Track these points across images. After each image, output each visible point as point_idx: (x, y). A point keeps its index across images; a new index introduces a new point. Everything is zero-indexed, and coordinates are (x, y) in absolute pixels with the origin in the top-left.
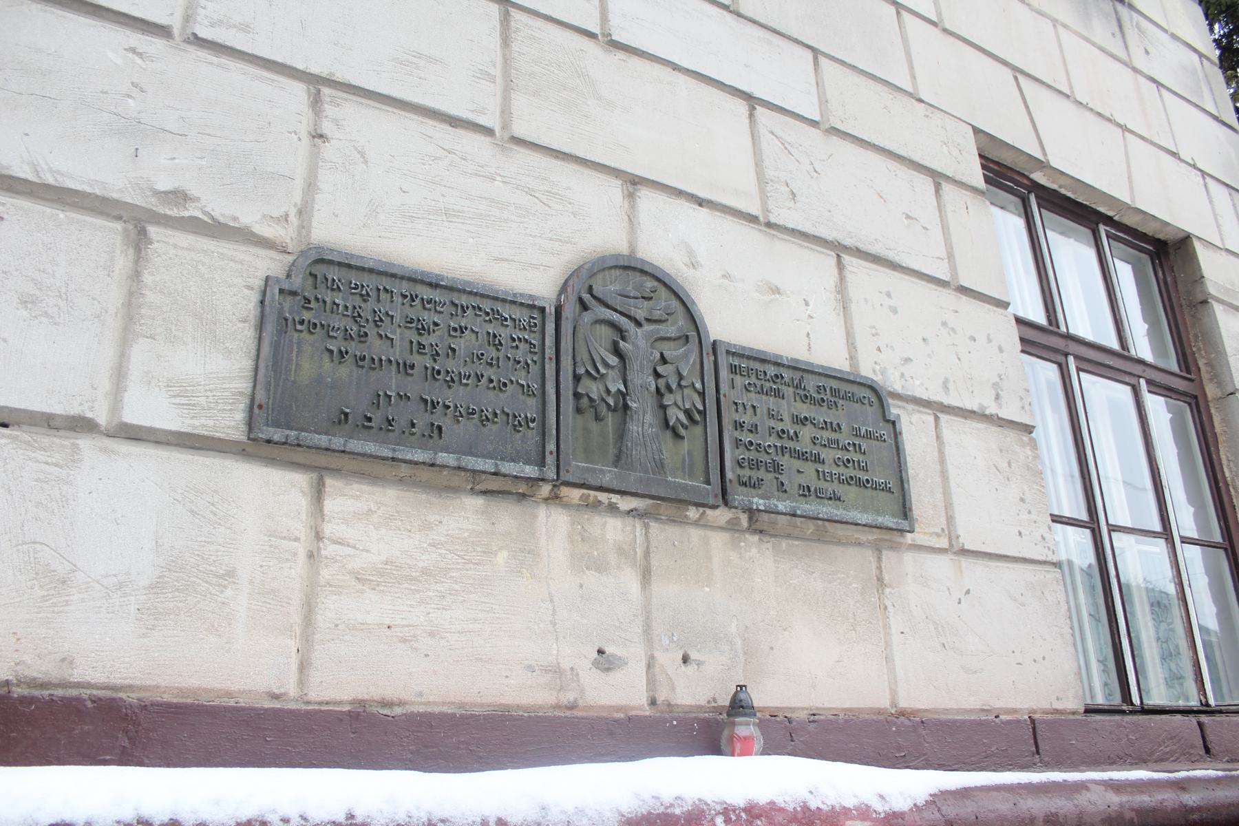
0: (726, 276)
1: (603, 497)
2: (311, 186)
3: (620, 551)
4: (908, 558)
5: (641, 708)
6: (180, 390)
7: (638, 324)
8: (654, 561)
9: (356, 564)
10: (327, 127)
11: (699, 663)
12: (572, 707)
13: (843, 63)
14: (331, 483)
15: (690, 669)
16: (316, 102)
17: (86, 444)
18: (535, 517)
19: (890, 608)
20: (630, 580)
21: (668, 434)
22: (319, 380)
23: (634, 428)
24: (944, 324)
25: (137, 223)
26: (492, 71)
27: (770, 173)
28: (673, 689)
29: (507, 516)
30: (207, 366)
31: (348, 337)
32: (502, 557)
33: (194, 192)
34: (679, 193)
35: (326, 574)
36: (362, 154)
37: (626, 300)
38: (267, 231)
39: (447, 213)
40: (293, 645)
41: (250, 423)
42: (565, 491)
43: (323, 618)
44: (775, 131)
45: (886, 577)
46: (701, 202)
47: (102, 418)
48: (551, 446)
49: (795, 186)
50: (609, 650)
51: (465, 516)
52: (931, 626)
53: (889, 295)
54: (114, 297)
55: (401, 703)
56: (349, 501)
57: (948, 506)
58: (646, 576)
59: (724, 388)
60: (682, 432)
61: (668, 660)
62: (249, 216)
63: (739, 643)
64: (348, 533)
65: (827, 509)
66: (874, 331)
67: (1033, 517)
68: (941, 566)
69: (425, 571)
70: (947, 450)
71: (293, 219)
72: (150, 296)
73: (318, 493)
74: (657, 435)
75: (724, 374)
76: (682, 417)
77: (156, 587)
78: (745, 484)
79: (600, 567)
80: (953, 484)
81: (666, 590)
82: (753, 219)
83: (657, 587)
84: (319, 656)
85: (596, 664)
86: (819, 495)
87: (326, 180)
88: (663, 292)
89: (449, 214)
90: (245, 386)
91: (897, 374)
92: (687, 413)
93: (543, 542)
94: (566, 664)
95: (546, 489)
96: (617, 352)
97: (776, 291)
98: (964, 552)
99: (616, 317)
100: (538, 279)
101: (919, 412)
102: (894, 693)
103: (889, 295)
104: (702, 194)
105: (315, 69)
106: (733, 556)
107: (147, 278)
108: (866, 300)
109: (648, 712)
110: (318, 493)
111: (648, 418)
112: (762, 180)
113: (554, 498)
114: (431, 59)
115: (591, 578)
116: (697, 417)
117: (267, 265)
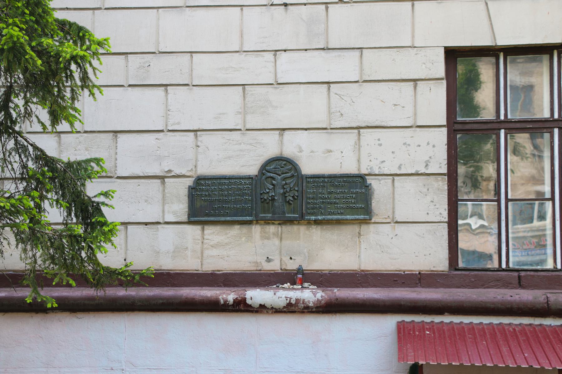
0: (312, 152)
2: (197, 160)
3: (274, 234)
4: (372, 227)
6: (174, 213)
7: (280, 175)
8: (283, 235)
9: (211, 244)
10: (199, 144)
11: (294, 259)
12: (260, 270)
13: (375, 48)
14: (206, 227)
15: (291, 261)
16: (196, 136)
17: (159, 226)
18: (252, 228)
19: (362, 242)
20: (276, 241)
21: (287, 204)
22: (201, 206)
23: (276, 204)
24: (405, 144)
25: (162, 178)
26: (240, 111)
27: (332, 110)
28: (287, 266)
29: (245, 229)
30: (179, 208)
31: (206, 196)
32: (243, 239)
33: (172, 169)
35: (205, 246)
36: (207, 148)
38: (188, 174)
39: (229, 158)
40: (199, 261)
41: (189, 218)
42: (259, 222)
43: (205, 255)
44: (337, 93)
45: (362, 233)
46: (306, 129)
47: (161, 222)
48: (254, 212)
49: (342, 112)
51: (236, 230)
52: (378, 246)
53: (379, 140)
54: (160, 196)
56: (210, 230)
57: (393, 208)
58: (281, 239)
59: (304, 188)
60: (291, 202)
61: (286, 259)
62: (184, 172)
63: (307, 254)
64: (210, 237)
65: (339, 217)
67: (436, 207)
69: (226, 244)
70: (396, 190)
71: (194, 169)
72: (167, 195)
73: (203, 230)
74: (283, 205)
75: (304, 184)
76: (291, 198)
77: (174, 252)
78: (309, 214)
79: (268, 238)
80: (396, 201)
81: (286, 243)
82: (326, 129)
83: (283, 242)
84: (204, 262)
85: (266, 261)
86: (333, 214)
87: (200, 157)
88: (288, 164)
89: (229, 158)
90: (187, 210)
91: (377, 168)
92: (293, 197)
94: (259, 261)
95: (255, 222)
96: (273, 185)
97: (330, 151)
98: (397, 222)
99: (272, 175)
100: (252, 170)
102: (360, 265)
103: (379, 140)
104: (305, 127)
105: (195, 129)
106: (307, 232)
107: (166, 191)
108: (368, 145)
110: (203, 230)
111: (280, 200)
112: (330, 113)
113: (257, 223)
114: (224, 114)
115: (266, 241)
116: (296, 197)
117: (189, 182)
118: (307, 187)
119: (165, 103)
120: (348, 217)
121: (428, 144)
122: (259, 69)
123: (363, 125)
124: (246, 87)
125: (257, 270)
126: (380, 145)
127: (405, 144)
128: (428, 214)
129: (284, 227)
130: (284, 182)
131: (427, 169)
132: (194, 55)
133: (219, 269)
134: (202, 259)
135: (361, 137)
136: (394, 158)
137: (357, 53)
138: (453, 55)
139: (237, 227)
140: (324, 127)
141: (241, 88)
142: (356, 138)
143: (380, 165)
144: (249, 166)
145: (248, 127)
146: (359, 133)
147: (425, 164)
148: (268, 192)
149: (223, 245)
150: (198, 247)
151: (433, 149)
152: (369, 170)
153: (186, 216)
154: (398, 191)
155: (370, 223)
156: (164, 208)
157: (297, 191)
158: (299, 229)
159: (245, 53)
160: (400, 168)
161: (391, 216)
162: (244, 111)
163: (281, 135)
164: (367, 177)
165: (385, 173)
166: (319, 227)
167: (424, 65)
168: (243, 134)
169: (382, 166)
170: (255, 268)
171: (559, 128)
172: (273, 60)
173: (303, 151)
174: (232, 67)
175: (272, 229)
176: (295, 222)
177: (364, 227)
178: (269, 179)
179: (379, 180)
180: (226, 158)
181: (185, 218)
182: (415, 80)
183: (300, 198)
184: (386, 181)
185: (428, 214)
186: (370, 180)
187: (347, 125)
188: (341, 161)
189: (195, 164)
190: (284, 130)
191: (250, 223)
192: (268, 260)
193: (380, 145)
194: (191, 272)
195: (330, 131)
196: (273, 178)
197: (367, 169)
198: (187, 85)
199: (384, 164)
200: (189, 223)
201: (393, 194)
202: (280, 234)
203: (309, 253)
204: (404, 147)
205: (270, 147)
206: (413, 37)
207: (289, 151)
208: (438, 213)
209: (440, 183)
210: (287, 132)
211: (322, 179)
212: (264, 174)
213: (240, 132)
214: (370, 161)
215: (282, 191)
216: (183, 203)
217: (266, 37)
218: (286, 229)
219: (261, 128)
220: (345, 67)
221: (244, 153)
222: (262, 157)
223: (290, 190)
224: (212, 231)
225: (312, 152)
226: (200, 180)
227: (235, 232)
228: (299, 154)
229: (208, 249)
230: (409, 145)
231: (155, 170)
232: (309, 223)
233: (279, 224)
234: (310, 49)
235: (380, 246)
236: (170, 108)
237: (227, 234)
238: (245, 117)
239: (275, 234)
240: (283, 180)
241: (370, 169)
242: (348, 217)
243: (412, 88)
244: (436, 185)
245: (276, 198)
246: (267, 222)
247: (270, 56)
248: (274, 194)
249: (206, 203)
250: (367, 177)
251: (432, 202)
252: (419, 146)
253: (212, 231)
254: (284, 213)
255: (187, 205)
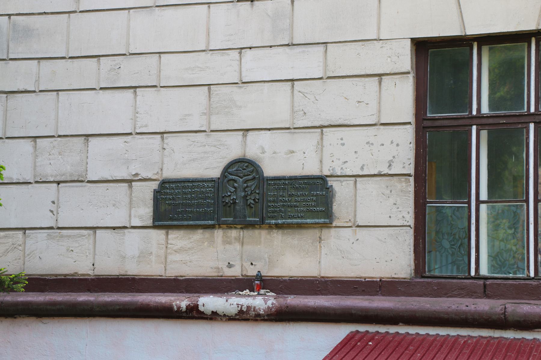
1: (232, 226)
2: (163, 164)
3: (235, 239)
4: (333, 231)
5: (239, 276)
6: (141, 217)
7: (241, 178)
8: (245, 240)
9: (175, 248)
10: (165, 146)
11: (255, 265)
12: (222, 276)
13: (340, 42)
14: (170, 232)
15: (251, 267)
16: (163, 138)
17: (126, 231)
18: (214, 233)
19: (323, 247)
20: (238, 246)
24: (368, 143)
25: (129, 182)
26: (205, 112)
27: (296, 109)
28: (247, 271)
29: (207, 233)
30: (144, 212)
32: (206, 244)
33: (139, 173)
34: (262, 129)
35: (169, 251)
36: (173, 150)
37: (243, 169)
39: (194, 160)
40: (163, 266)
41: (153, 222)
42: (221, 226)
43: (168, 260)
44: (301, 90)
45: (323, 238)
46: (269, 129)
47: (128, 226)
48: (216, 216)
50: (231, 263)
51: (198, 235)
52: (339, 252)
53: (342, 139)
54: (127, 200)
55: (184, 276)
56: (174, 235)
57: (355, 211)
59: (265, 190)
60: (253, 206)
61: (247, 265)
62: (150, 175)
63: (267, 260)
65: (299, 221)
66: (332, 155)
68: (347, 232)
69: (189, 248)
70: (358, 192)
71: (160, 172)
72: (134, 199)
73: (167, 234)
75: (265, 187)
76: (252, 202)
77: (139, 257)
78: (269, 217)
79: (230, 243)
80: (358, 203)
82: (289, 128)
83: (245, 247)
85: (227, 266)
87: (166, 160)
88: (250, 166)
89: (194, 160)
90: (152, 214)
91: (339, 169)
92: (254, 200)
93: (216, 239)
94: (220, 267)
96: (235, 188)
97: (293, 152)
98: (358, 226)
99: (234, 177)
100: (215, 173)
101: (346, 180)
102: (320, 271)
103: (342, 139)
104: (268, 127)
105: (162, 131)
106: (268, 237)
107: (133, 195)
108: (330, 144)
109: (241, 277)
110: (167, 234)
112: (293, 112)
113: (220, 227)
114: (189, 115)
115: (228, 246)
116: (257, 201)
117: (155, 185)
118: (268, 190)
119: (134, 105)
120: (309, 221)
121: (392, 142)
122: (224, 68)
123: (326, 124)
124: (212, 86)
125: (218, 276)
126: (343, 144)
127: (368, 143)
128: (390, 217)
129: (245, 231)
130: (246, 185)
131: (390, 170)
132: (162, 55)
133: (182, 274)
134: (166, 264)
135: (324, 136)
136: (357, 158)
137: (321, 48)
138: (421, 46)
139: (200, 231)
140: (287, 126)
141: (206, 87)
142: (319, 138)
143: (342, 166)
144: (210, 167)
145: (213, 128)
146: (322, 133)
147: (388, 164)
148: (230, 196)
149: (186, 250)
150: (162, 252)
151: (399, 149)
152: (332, 171)
153: (152, 221)
154: (360, 192)
155: (331, 227)
156: (130, 212)
157: (259, 194)
158: (260, 234)
159: (211, 52)
160: (362, 168)
161: (352, 220)
162: (209, 112)
163: (245, 136)
164: (328, 179)
165: (347, 174)
166: (280, 231)
167: (389, 59)
168: (208, 135)
169: (344, 166)
170: (216, 274)
171: (535, 122)
172: (238, 58)
173: (265, 152)
174: (198, 67)
175: (234, 233)
176: (256, 226)
177: (325, 231)
178: (232, 182)
179: (341, 182)
180: (190, 161)
181: (150, 222)
182: (380, 75)
183: (261, 201)
184: (348, 182)
185: (390, 217)
186: (331, 182)
187: (310, 125)
188: (304, 162)
189: (161, 167)
190: (248, 130)
191: (212, 227)
192: (230, 266)
193: (343, 144)
194: (155, 277)
195: (293, 131)
196: (235, 181)
197: (329, 170)
198: (155, 86)
199: (346, 164)
200: (154, 227)
201: (356, 196)
202: (241, 238)
203: (269, 258)
204: (367, 146)
205: (232, 149)
206: (379, 29)
207: (252, 153)
208: (401, 216)
209: (404, 184)
210: (250, 133)
211: (283, 181)
212: (226, 177)
213: (205, 133)
214: (333, 161)
215: (243, 194)
216: (149, 207)
217: (232, 35)
218: (248, 233)
219: (225, 129)
220: (309, 63)
221: (208, 155)
222: (226, 159)
223: (251, 193)
224: (176, 236)
225: (275, 153)
226: (165, 184)
227: (198, 237)
228: (262, 155)
229: (171, 254)
230: (372, 144)
231: (123, 174)
232: (270, 227)
233: (242, 228)
234: (275, 46)
235: (341, 251)
236: (138, 110)
237: (190, 238)
238: (210, 118)
239: (238, 239)
240: (245, 183)
241: (333, 170)
242: (309, 221)
243: (377, 83)
244: (399, 186)
245: (237, 201)
246: (230, 226)
247: (235, 54)
248: (235, 197)
249: (170, 207)
250: (328, 179)
251: (395, 204)
252: (383, 145)
253: (176, 236)
254: (245, 217)
255: (152, 209)
